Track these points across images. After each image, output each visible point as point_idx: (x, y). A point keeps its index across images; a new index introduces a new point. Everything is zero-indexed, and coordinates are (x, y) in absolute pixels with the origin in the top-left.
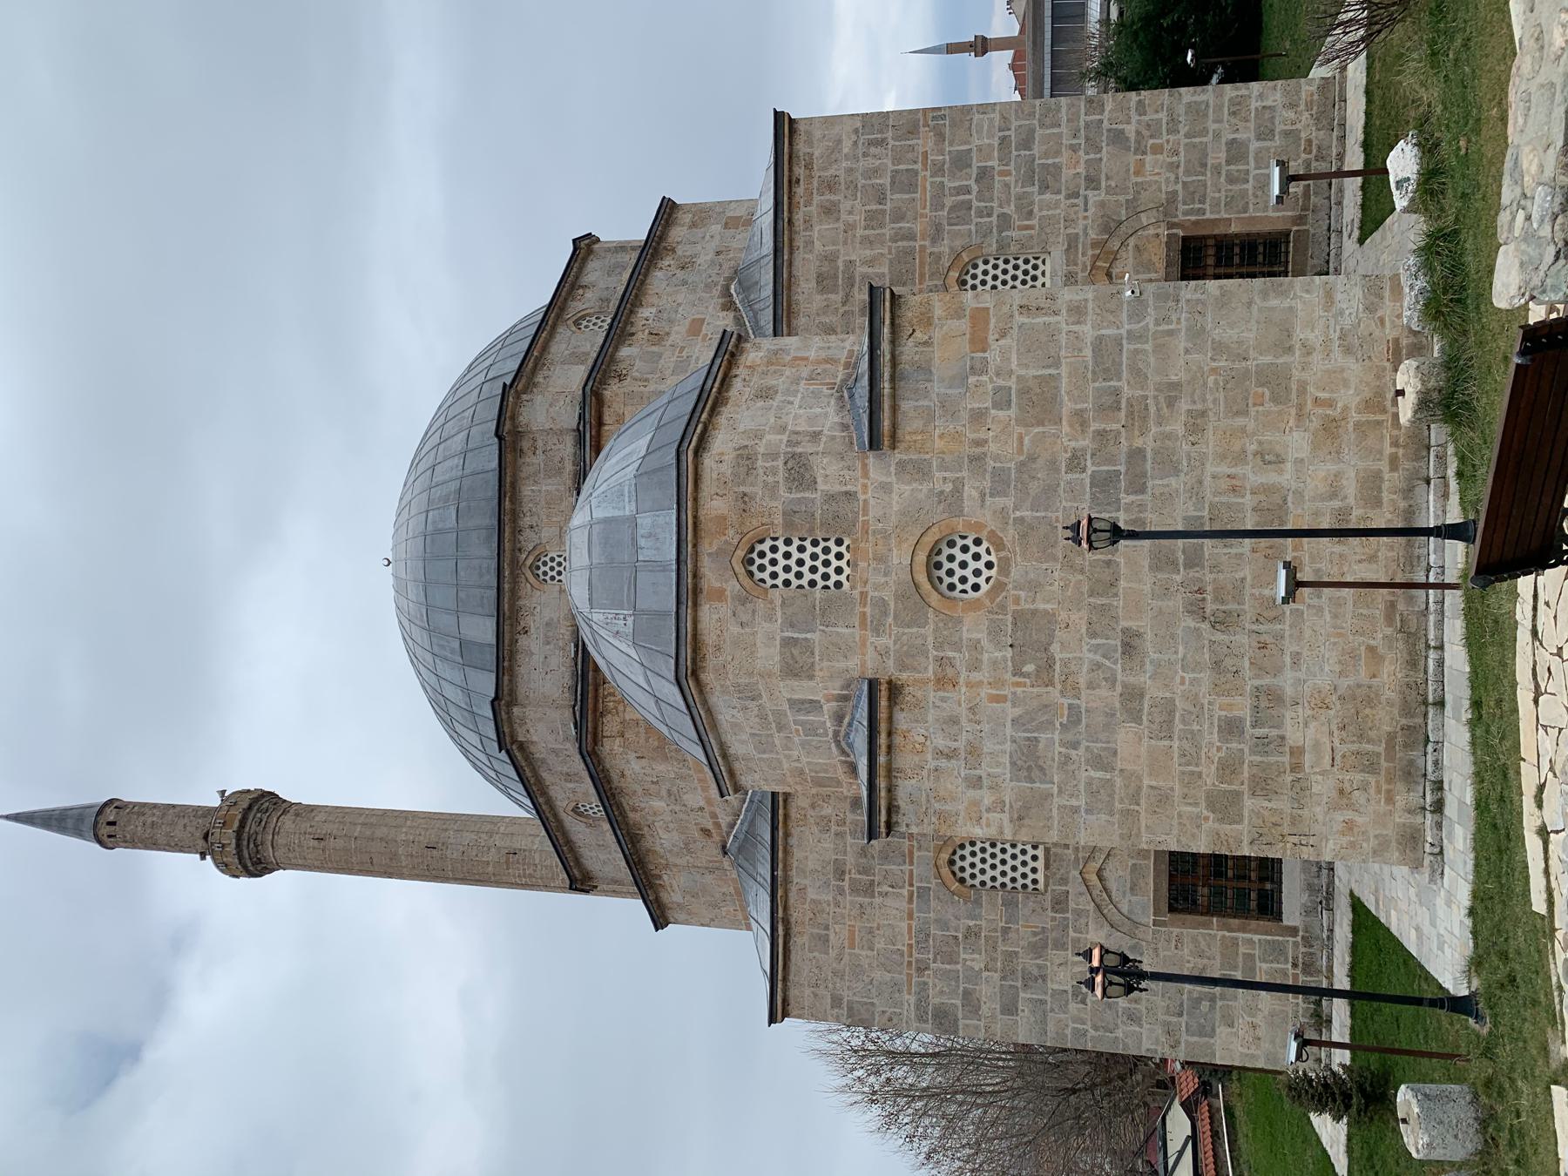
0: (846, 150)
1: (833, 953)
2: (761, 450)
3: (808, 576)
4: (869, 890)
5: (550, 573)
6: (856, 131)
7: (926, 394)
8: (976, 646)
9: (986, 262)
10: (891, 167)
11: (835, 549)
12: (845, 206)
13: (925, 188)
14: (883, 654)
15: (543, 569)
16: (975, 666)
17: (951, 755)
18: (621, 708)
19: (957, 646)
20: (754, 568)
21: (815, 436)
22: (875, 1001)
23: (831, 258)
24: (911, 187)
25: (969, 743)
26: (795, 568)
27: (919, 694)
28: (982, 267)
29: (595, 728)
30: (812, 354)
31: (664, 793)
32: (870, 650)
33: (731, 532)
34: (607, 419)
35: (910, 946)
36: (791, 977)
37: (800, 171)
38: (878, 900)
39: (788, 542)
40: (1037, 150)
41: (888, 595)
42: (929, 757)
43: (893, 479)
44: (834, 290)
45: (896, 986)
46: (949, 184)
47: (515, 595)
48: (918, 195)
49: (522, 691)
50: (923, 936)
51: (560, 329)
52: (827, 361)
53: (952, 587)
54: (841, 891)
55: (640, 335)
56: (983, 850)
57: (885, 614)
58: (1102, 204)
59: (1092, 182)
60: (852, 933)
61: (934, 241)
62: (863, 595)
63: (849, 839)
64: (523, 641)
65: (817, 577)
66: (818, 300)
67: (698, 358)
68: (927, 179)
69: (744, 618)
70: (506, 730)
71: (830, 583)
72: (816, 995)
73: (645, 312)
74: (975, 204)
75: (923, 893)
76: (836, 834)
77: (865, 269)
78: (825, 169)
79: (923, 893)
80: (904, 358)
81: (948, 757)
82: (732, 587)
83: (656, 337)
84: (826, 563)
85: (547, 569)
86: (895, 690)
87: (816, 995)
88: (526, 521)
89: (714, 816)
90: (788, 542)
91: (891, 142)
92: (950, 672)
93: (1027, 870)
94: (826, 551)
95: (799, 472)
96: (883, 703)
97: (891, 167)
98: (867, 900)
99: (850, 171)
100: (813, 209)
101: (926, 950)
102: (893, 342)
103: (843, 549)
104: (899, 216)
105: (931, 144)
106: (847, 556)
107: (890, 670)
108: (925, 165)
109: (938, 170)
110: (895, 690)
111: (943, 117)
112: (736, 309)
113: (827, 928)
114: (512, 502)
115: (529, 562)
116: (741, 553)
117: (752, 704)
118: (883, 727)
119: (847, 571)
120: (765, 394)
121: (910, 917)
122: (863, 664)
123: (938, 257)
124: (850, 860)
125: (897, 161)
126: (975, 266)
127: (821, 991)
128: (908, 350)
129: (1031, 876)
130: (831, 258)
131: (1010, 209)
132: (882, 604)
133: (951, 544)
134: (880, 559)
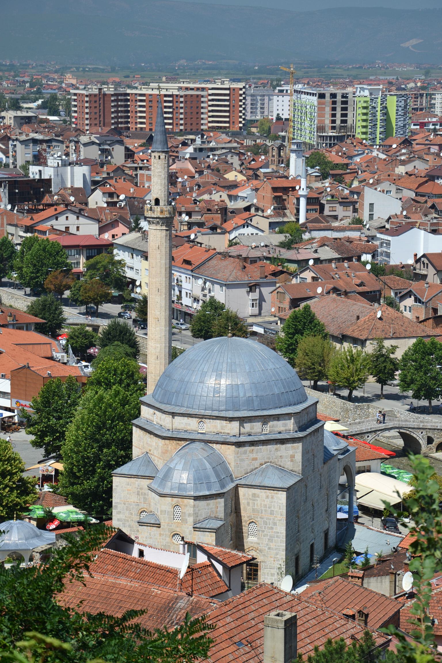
8: (165, 539)
12: (268, 500)
14: (164, 526)
16: (163, 539)
23: (258, 497)
24: (271, 514)
37: (275, 492)
40: (276, 538)
44: (252, 496)
47: (195, 417)
58: (265, 550)
59: (269, 548)
61: (260, 518)
64: (186, 418)
66: (250, 493)
75: (138, 505)
77: (256, 502)
79: (138, 505)
104: (266, 511)
105: (279, 518)
123: (257, 518)
125: (276, 511)
130: (258, 497)
131: (265, 533)
132: (171, 526)
134: (178, 527)
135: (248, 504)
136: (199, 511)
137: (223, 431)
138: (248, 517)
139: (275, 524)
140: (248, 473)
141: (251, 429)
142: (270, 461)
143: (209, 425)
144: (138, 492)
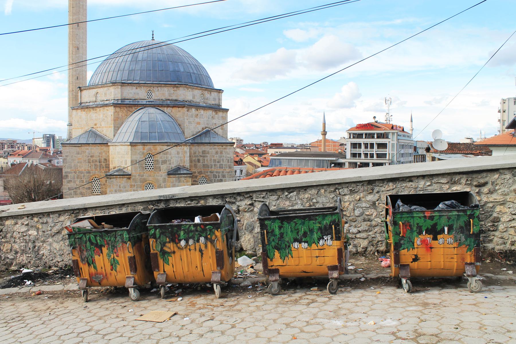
0: (227, 155)
1: (76, 155)
2: (168, 156)
3: (147, 164)
4: (89, 162)
5: (149, 94)
6: (230, 157)
7: (176, 182)
9: (206, 181)
10: (224, 164)
11: (152, 168)
12: (217, 155)
13: (219, 170)
14: (135, 176)
15: (150, 92)
17: (120, 187)
18: (122, 112)
19: (137, 188)
20: (148, 155)
21: (170, 164)
22: (68, 164)
23: (208, 153)
24: (220, 168)
25: (122, 190)
26: (148, 162)
27: (129, 182)
28: (205, 180)
29: (117, 106)
30: (186, 159)
31: (104, 118)
32: (136, 174)
33: (154, 151)
34: (179, 108)
35: (79, 170)
36: (70, 147)
37: (224, 147)
38: (87, 164)
39: (153, 160)
41: (145, 177)
42: (119, 184)
43: (163, 177)
44: (203, 154)
45: (71, 168)
46: (220, 174)
48: (218, 169)
49: (124, 87)
50: (82, 173)
51: (201, 91)
52: (184, 162)
53: (146, 186)
54: (88, 157)
55: (197, 112)
56: (98, 183)
57: (141, 177)
60: (80, 159)
61: (211, 172)
62: (144, 173)
63: (98, 158)
64: (135, 88)
65: (147, 165)
66: (201, 151)
67: (191, 125)
68: (221, 170)
69: (140, 154)
70: (116, 84)
71: (146, 167)
72: (67, 152)
73: (202, 112)
74: (216, 179)
75: (89, 173)
76: (99, 156)
77: (206, 158)
78: (224, 152)
79: (89, 173)
80: (181, 178)
81: (119, 187)
82: (145, 151)
84: (149, 167)
85: (150, 93)
86: (129, 178)
87: (67, 152)
88: (159, 88)
89: (100, 127)
90: (153, 160)
91: (228, 164)
92: (133, 187)
93: (96, 191)
94: (151, 167)
95: (164, 162)
96: (127, 177)
97: (224, 164)
98: (87, 162)
99: (224, 156)
100: (217, 150)
101: (79, 173)
102: (184, 177)
103: (152, 169)
104: (215, 165)
105: (227, 171)
106: (151, 170)
107: (133, 178)
108: (224, 170)
109: (223, 172)
110: (129, 178)
111: (232, 173)
112: (202, 131)
113: (81, 154)
114: (164, 86)
115: (151, 89)
116: (151, 153)
117: (126, 153)
118: (123, 177)
119: (148, 170)
120: (178, 153)
121: (85, 170)
122: (134, 173)
124: (94, 158)
126: (206, 179)
127: (68, 153)
128: (183, 179)
129: (94, 192)
130: (208, 153)
132: (143, 176)
133: (153, 186)
134: (150, 176)
135: (199, 161)
137: (170, 98)
138: (199, 173)
140: (194, 135)
141: (193, 98)
142: (208, 126)
143: (157, 93)
144: (89, 159)
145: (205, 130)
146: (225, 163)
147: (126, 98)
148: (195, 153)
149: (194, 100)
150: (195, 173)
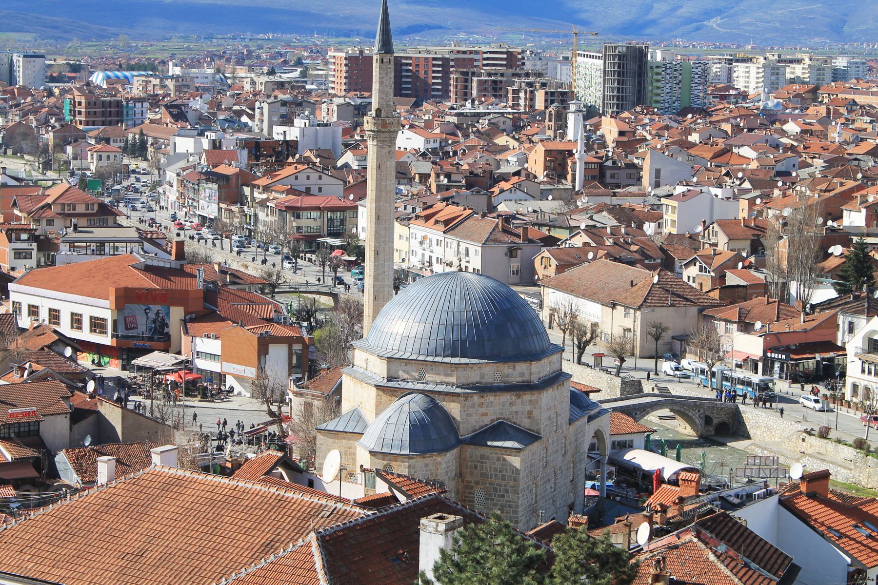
23: (488, 459)
24: (502, 479)
30: (439, 471)
40: (508, 509)
44: (481, 458)
66: (479, 454)
68: (503, 483)
83: (481, 405)
104: (496, 475)
109: (505, 486)
120: (427, 465)
130: (488, 459)
135: (476, 467)
136: (415, 472)
139: (507, 491)
140: (476, 431)
145: (495, 423)
146: (509, 474)
147: (394, 376)
148: (471, 457)
149: (483, 381)
150: (471, 482)
